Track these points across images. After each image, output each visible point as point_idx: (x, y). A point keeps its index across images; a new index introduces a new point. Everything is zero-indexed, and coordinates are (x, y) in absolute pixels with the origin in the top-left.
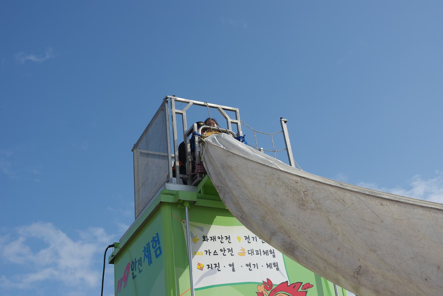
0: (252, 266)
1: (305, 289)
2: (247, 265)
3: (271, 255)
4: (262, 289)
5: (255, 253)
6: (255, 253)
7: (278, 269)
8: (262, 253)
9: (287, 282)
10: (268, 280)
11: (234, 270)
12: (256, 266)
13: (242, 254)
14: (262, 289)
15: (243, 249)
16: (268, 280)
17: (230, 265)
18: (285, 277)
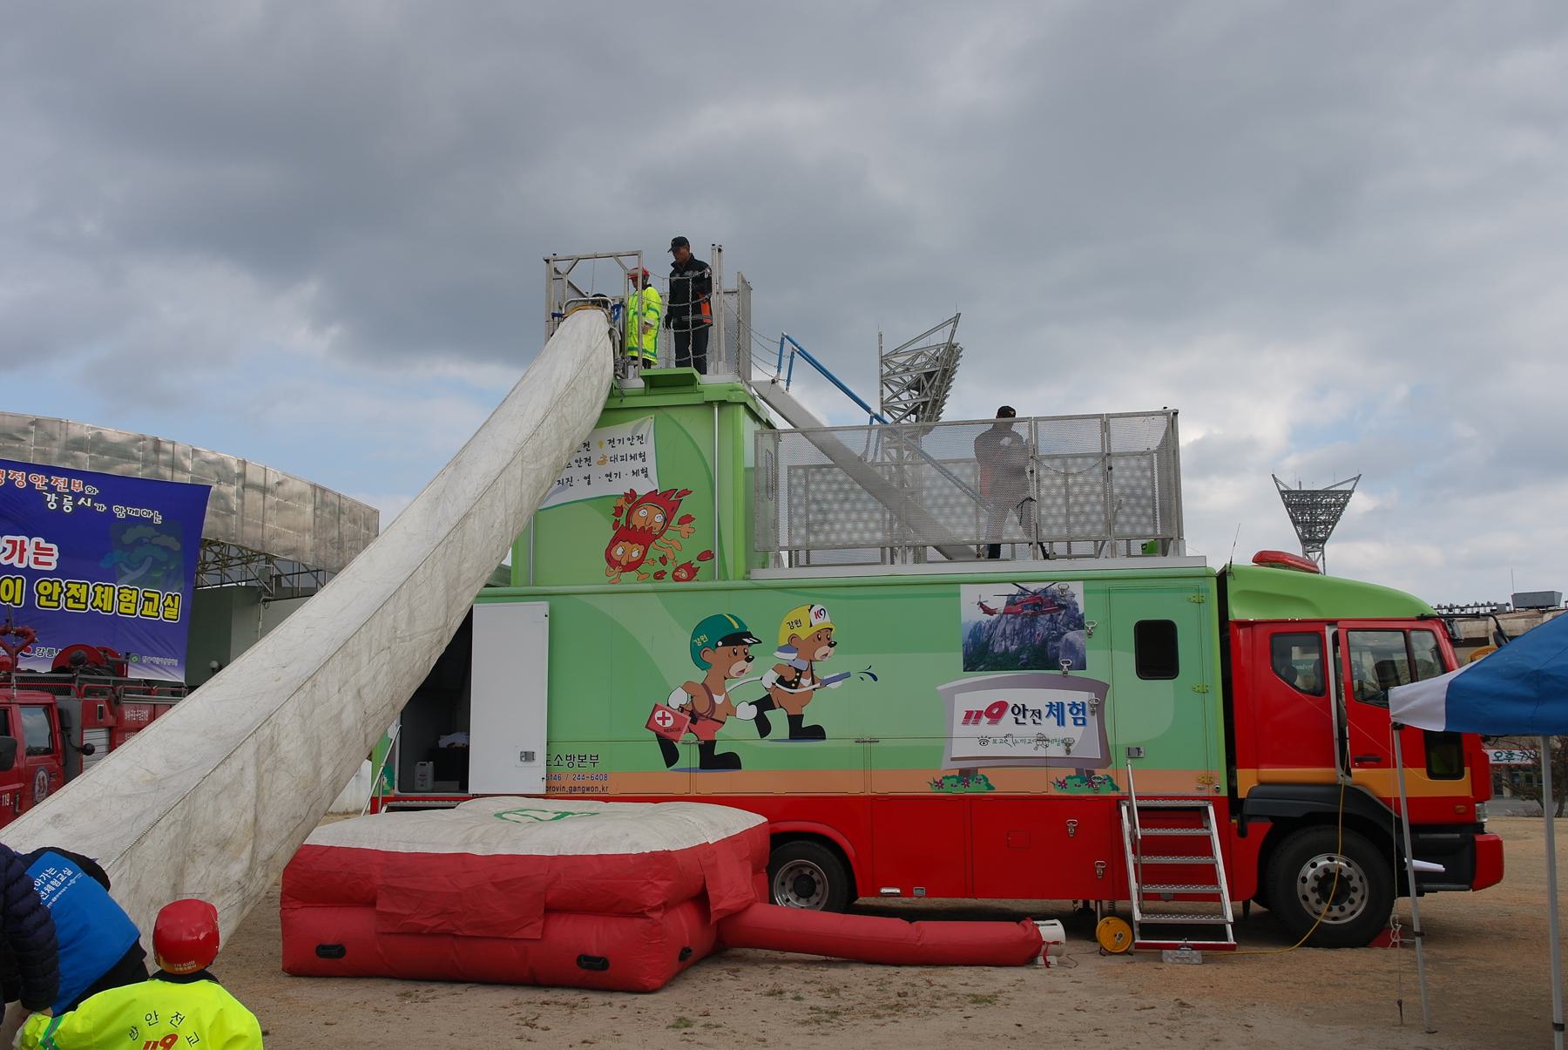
0: (613, 476)
1: (680, 497)
2: (607, 476)
3: (640, 460)
4: (622, 503)
5: (619, 458)
6: (619, 458)
7: (646, 476)
8: (629, 458)
9: (656, 490)
10: (631, 490)
11: (589, 483)
12: (618, 475)
13: (603, 462)
14: (622, 503)
15: (604, 457)
16: (631, 490)
17: (585, 478)
18: (653, 483)
